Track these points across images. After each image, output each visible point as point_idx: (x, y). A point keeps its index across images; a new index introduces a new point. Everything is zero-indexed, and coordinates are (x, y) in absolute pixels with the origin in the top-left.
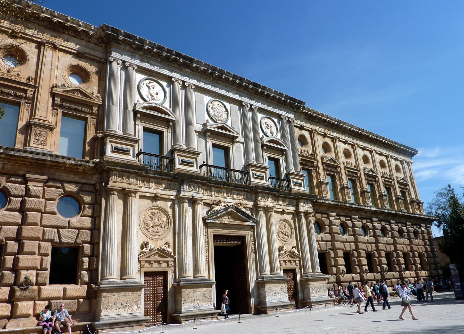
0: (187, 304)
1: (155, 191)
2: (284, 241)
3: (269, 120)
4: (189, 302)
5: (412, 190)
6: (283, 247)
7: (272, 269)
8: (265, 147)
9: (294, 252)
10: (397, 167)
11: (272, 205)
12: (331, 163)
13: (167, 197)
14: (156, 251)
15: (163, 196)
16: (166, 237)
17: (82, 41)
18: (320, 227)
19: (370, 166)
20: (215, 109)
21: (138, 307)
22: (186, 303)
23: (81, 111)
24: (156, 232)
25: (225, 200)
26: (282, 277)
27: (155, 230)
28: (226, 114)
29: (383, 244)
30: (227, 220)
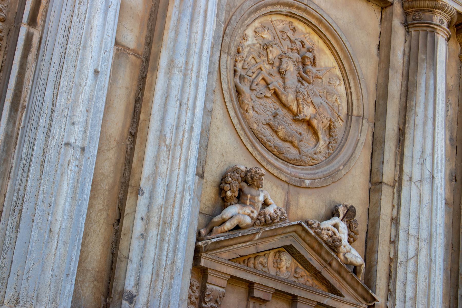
2: (279, 155)
6: (250, 180)
9: (334, 246)
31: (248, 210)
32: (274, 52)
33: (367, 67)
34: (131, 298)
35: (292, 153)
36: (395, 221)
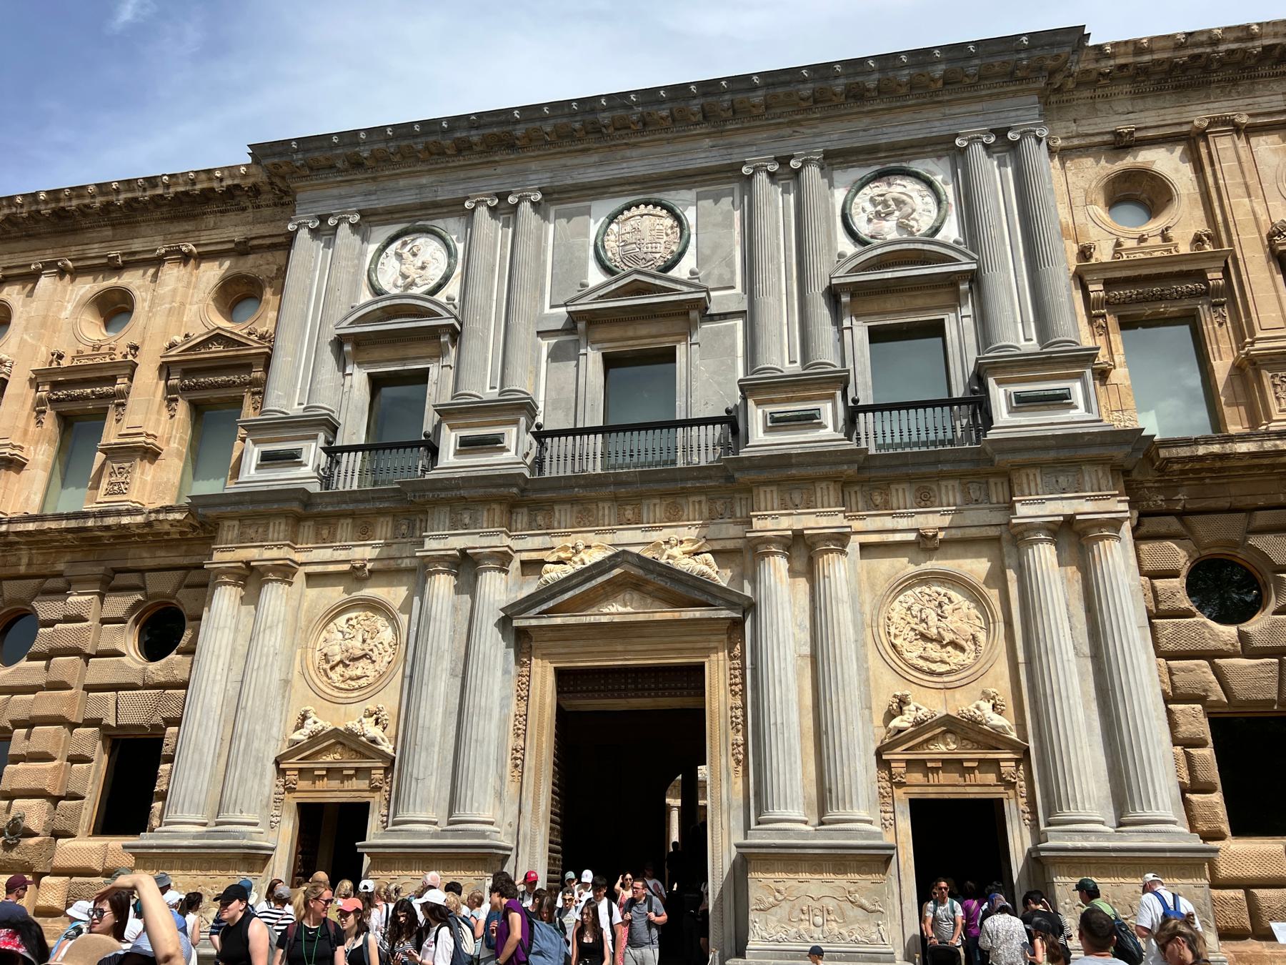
2: (932, 673)
7: (824, 798)
8: (845, 299)
17: (245, 214)
20: (627, 237)
24: (351, 679)
30: (615, 610)
31: (904, 717)
32: (916, 608)
35: (944, 668)
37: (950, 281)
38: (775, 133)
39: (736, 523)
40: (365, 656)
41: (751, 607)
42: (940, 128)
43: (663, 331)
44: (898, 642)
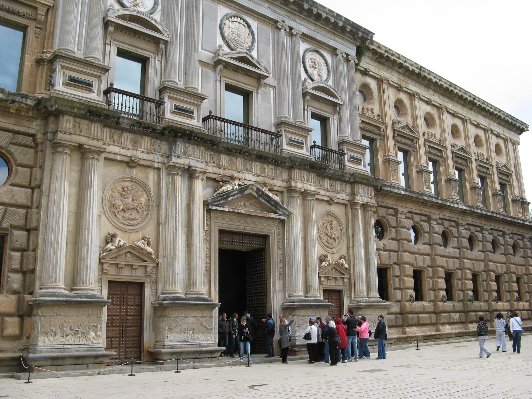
0: (174, 334)
1: (129, 153)
2: (329, 248)
3: (317, 55)
4: (177, 333)
5: (515, 183)
6: (326, 256)
8: (308, 98)
9: (342, 265)
10: (497, 146)
11: (313, 189)
12: (406, 131)
13: (149, 163)
14: (127, 250)
15: (142, 162)
16: (143, 228)
18: (381, 229)
19: (460, 143)
21: (96, 335)
22: (172, 333)
23: (18, 14)
24: (129, 219)
25: (240, 175)
26: (321, 301)
27: (127, 215)
28: (250, 39)
29: (471, 260)
32: (325, 225)
33: (343, 221)
34: (311, 286)
35: (332, 246)
36: (354, 255)
37: (335, 105)
38: (288, 15)
39: (283, 181)
40: (134, 208)
41: (289, 215)
42: (332, 43)
43: (248, 83)
44: (321, 236)
